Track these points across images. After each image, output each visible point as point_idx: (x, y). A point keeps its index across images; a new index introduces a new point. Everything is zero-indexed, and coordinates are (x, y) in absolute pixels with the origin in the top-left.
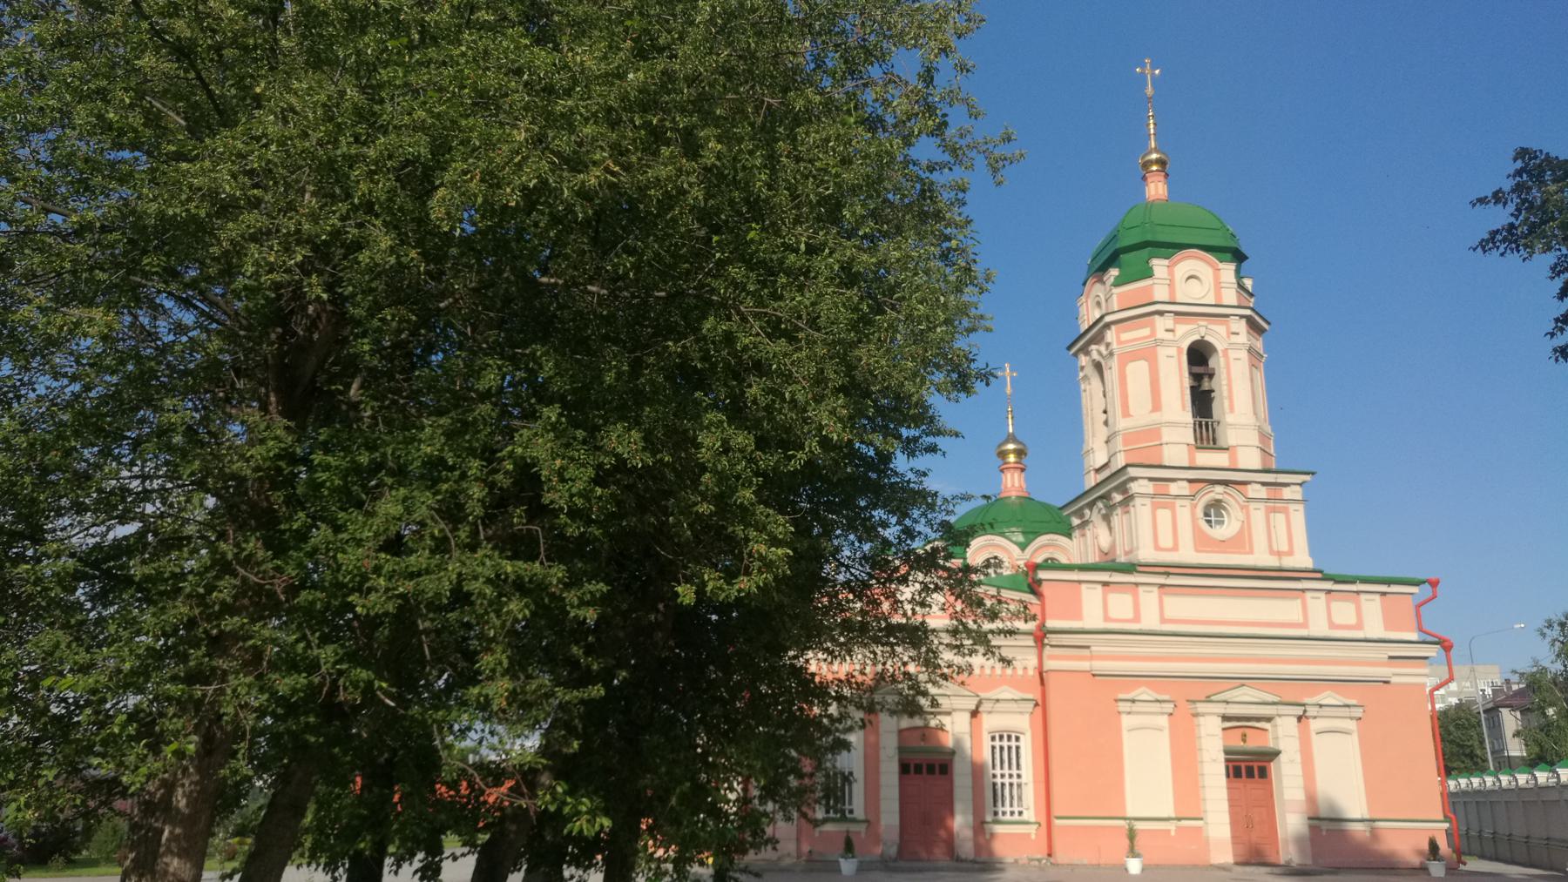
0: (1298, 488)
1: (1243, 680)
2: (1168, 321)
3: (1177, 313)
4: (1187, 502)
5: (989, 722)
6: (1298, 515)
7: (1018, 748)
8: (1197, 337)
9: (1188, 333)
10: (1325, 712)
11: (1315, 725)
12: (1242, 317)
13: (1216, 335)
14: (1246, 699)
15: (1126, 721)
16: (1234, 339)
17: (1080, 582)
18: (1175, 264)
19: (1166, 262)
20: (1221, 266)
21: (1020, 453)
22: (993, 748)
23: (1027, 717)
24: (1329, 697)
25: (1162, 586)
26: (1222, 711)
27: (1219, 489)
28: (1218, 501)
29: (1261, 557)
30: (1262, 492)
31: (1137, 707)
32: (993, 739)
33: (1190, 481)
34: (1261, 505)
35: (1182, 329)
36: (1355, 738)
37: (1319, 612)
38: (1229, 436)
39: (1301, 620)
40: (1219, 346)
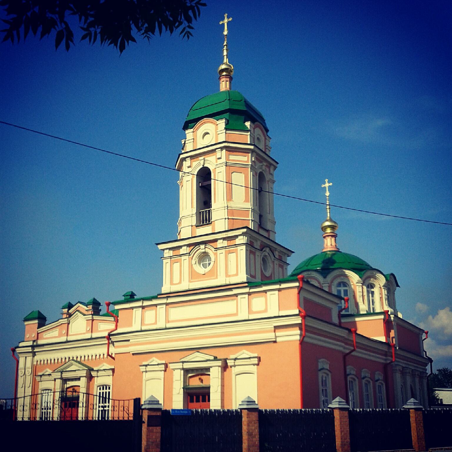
0: (242, 237)
1: (197, 349)
2: (188, 161)
3: (192, 157)
4: (186, 257)
5: (98, 381)
6: (242, 251)
7: (109, 392)
8: (201, 166)
9: (197, 165)
10: (238, 362)
11: (235, 370)
12: (222, 148)
13: (211, 162)
14: (197, 360)
15: (146, 376)
16: (220, 161)
17: (132, 308)
18: (197, 129)
19: (192, 130)
20: (218, 122)
21: (333, 227)
22: (100, 393)
23: (112, 376)
24: (245, 353)
25: (167, 304)
26: (181, 367)
27: (202, 246)
28: (205, 253)
29: (221, 280)
30: (225, 243)
31: (149, 368)
32: (100, 389)
33: (189, 245)
34: (223, 251)
35: (195, 164)
36: (255, 376)
37: (239, 306)
38: (214, 216)
39: (235, 312)
40: (211, 168)
